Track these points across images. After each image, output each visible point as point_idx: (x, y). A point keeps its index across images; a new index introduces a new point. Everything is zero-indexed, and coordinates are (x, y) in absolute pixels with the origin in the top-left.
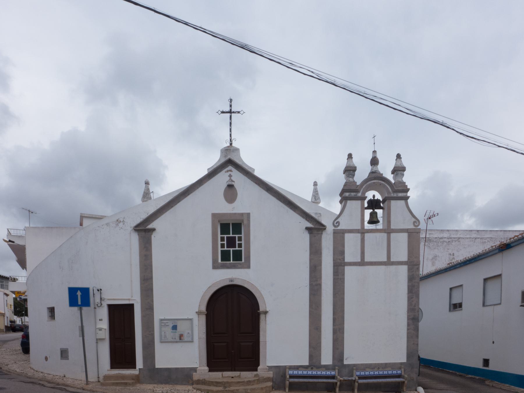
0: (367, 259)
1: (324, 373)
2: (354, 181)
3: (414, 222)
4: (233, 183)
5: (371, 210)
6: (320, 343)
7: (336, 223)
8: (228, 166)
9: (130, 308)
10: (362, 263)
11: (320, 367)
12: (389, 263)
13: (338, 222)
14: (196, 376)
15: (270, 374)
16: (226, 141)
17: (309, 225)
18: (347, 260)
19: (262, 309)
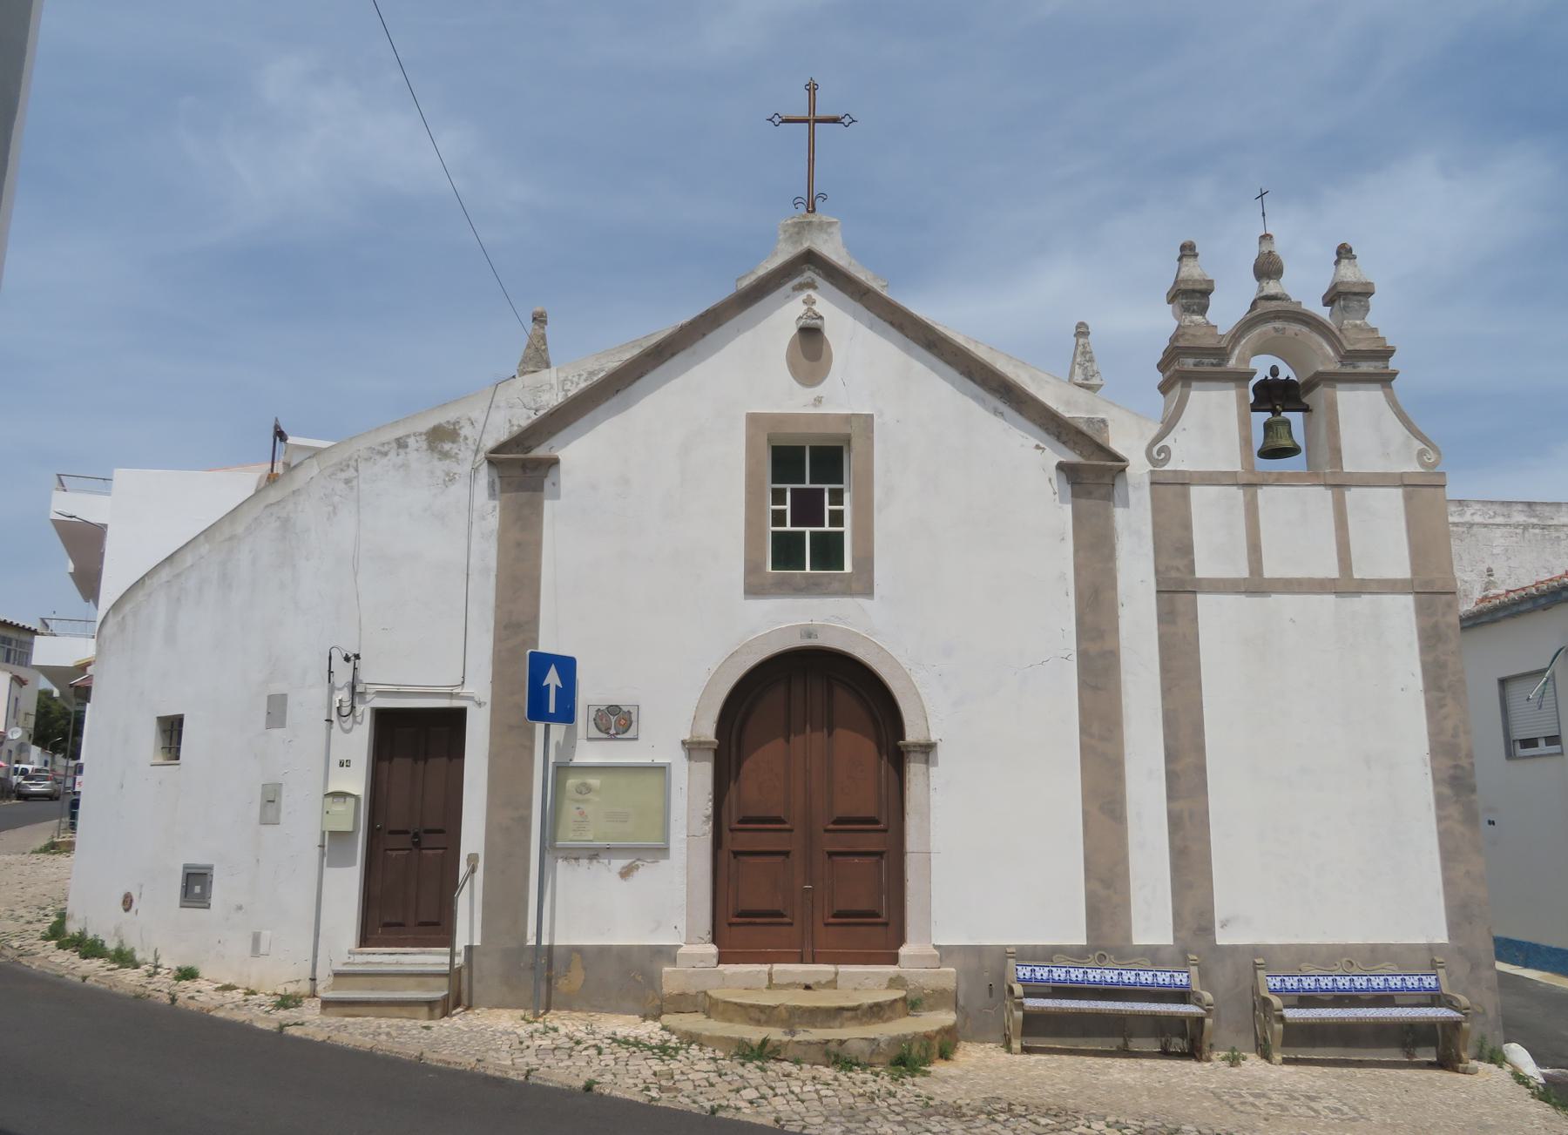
0: (1271, 570)
1: (1147, 977)
2: (1208, 323)
3: (1421, 453)
4: (819, 322)
5: (1268, 415)
6: (1124, 860)
7: (1157, 452)
8: (802, 272)
9: (451, 722)
10: (1256, 585)
11: (1125, 954)
12: (1346, 585)
13: (1165, 450)
14: (672, 979)
15: (947, 976)
16: (795, 202)
17: (1072, 457)
18: (1202, 571)
19: (912, 735)
